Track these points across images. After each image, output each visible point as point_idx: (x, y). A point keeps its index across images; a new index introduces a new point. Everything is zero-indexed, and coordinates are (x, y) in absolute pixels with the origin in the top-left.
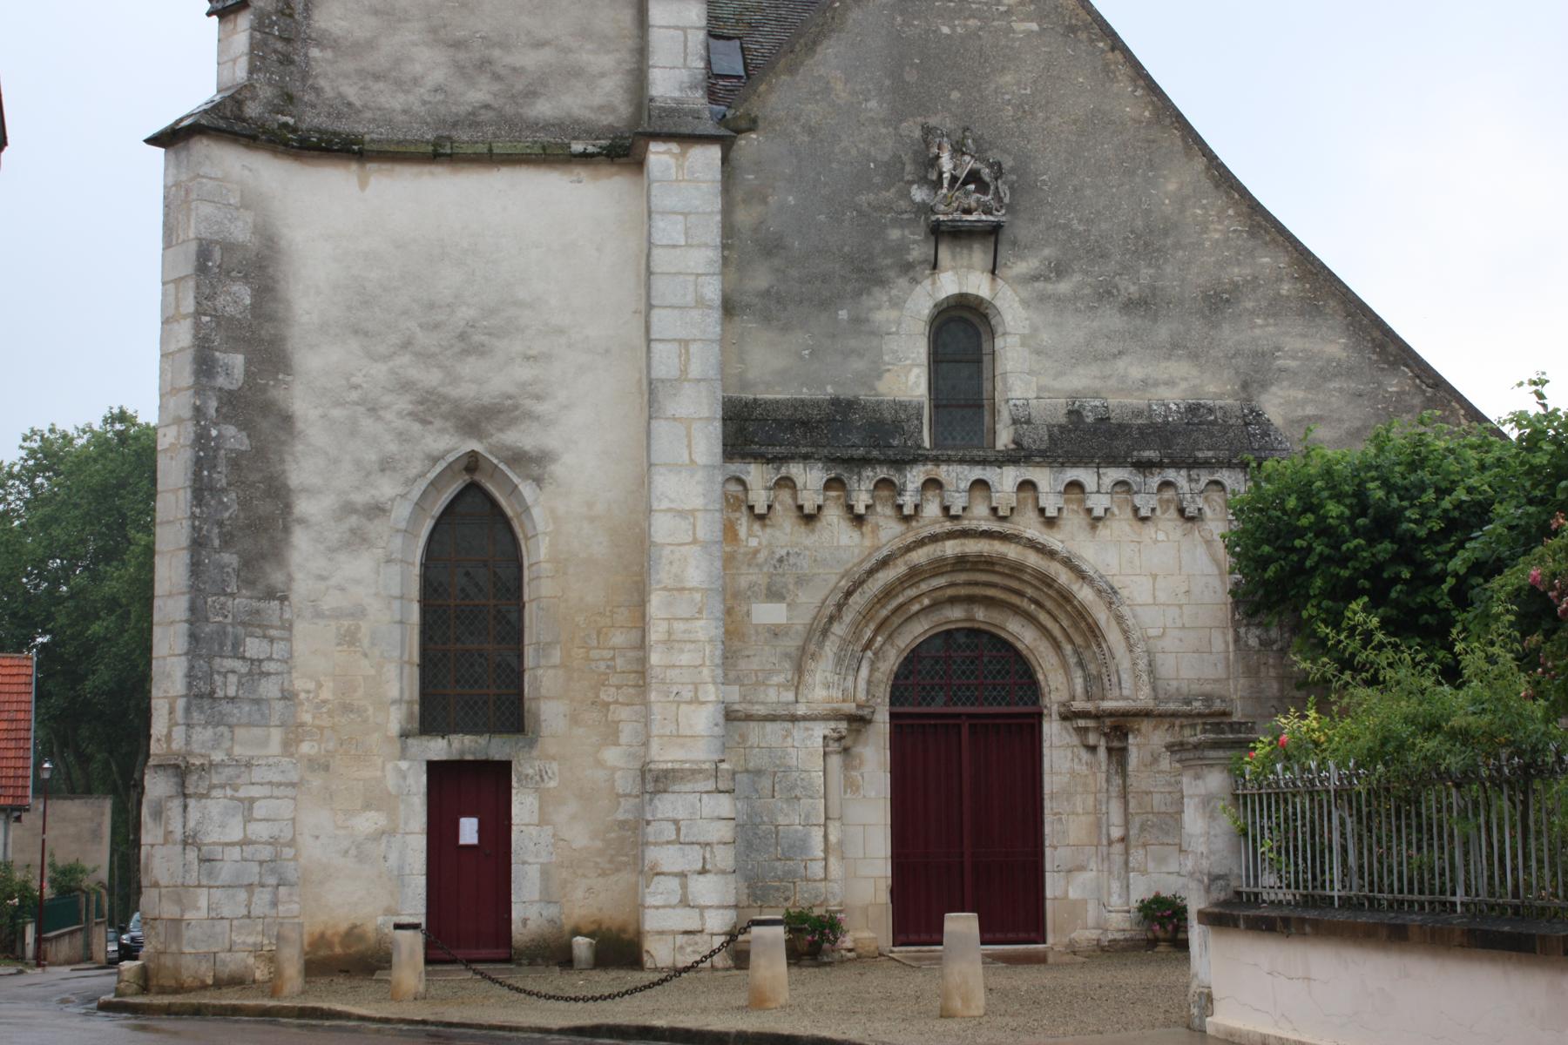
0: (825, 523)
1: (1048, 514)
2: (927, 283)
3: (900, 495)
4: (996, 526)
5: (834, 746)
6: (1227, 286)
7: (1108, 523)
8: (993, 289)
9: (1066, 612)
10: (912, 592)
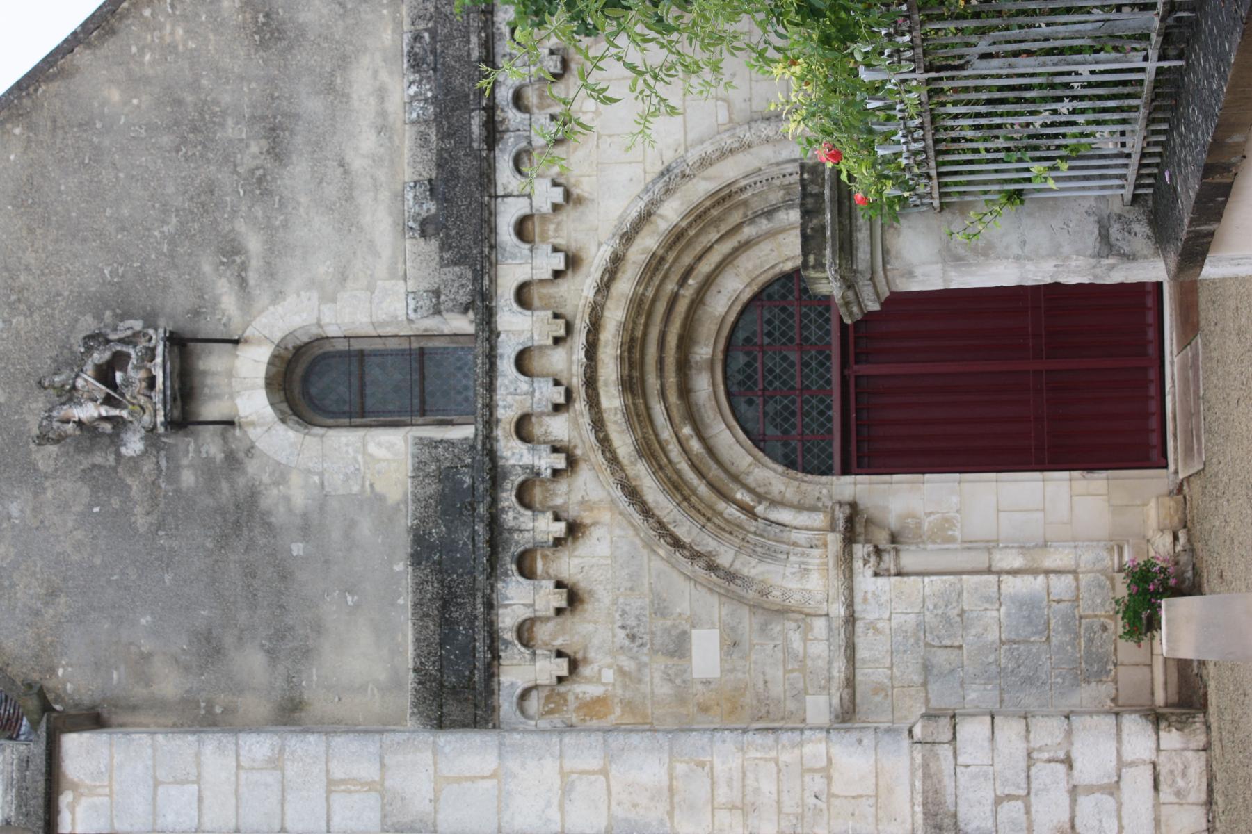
0: (580, 576)
1: (561, 266)
2: (253, 433)
3: (538, 474)
4: (580, 339)
5: (888, 561)
6: (248, 16)
7: (572, 180)
8: (259, 342)
9: (697, 235)
10: (674, 451)
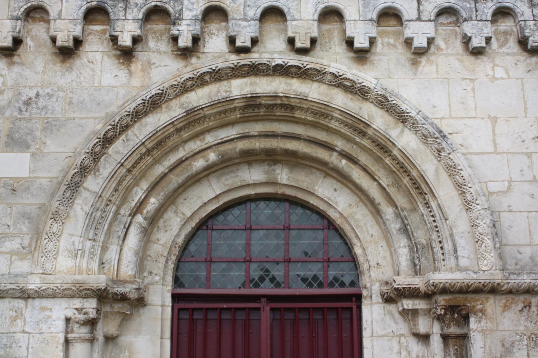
0: (85, 60)
1: (357, 45)
3: (174, 24)
4: (293, 60)
5: (83, 332)
7: (433, 58)
9: (386, 167)
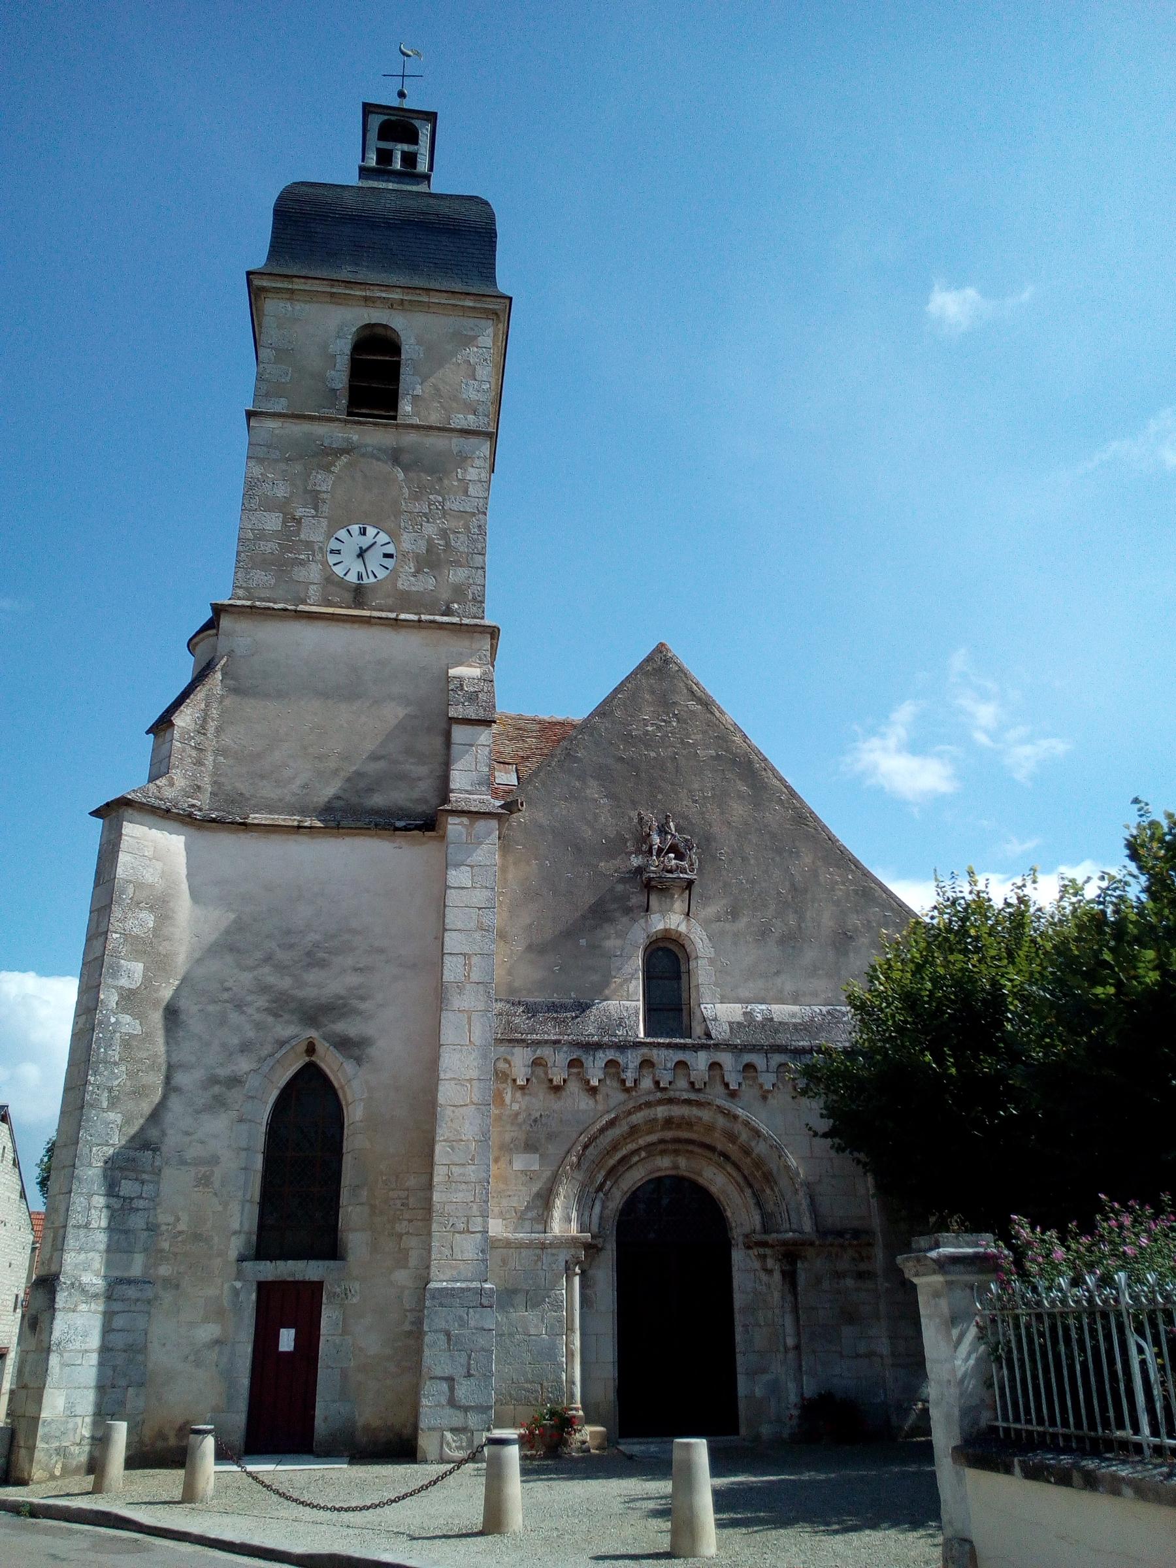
2: (642, 921)
4: (693, 1096)
6: (850, 927)
8: (687, 926)
10: (632, 1146)
